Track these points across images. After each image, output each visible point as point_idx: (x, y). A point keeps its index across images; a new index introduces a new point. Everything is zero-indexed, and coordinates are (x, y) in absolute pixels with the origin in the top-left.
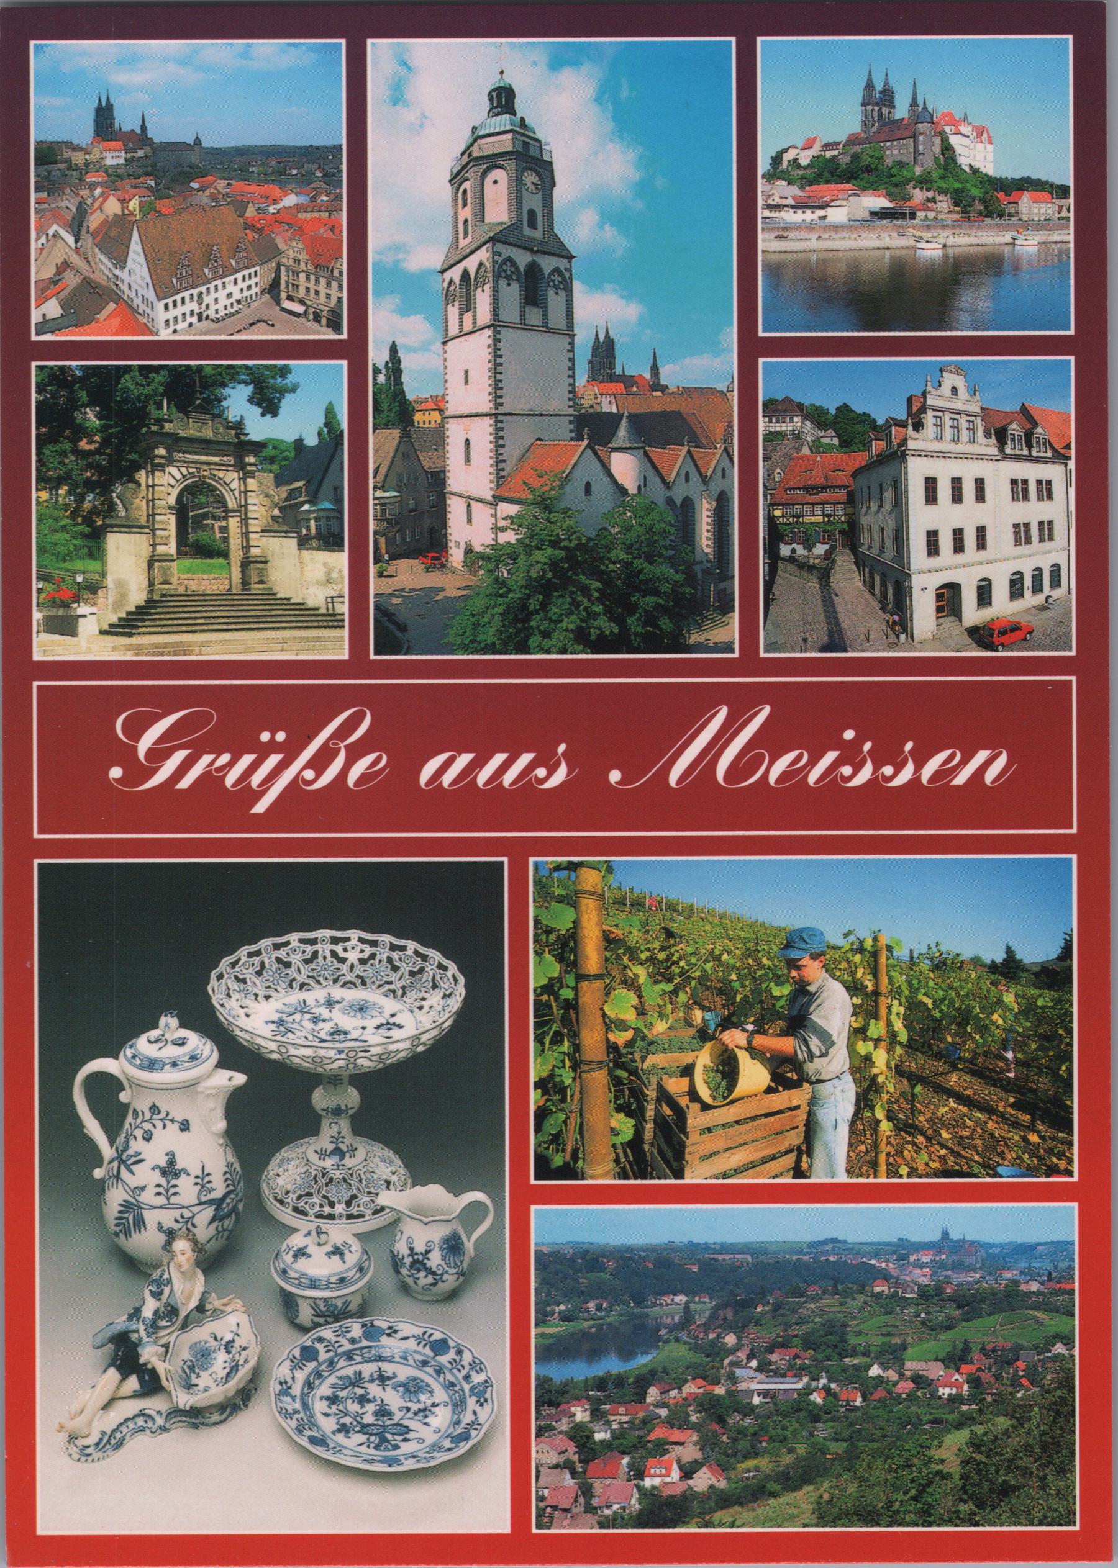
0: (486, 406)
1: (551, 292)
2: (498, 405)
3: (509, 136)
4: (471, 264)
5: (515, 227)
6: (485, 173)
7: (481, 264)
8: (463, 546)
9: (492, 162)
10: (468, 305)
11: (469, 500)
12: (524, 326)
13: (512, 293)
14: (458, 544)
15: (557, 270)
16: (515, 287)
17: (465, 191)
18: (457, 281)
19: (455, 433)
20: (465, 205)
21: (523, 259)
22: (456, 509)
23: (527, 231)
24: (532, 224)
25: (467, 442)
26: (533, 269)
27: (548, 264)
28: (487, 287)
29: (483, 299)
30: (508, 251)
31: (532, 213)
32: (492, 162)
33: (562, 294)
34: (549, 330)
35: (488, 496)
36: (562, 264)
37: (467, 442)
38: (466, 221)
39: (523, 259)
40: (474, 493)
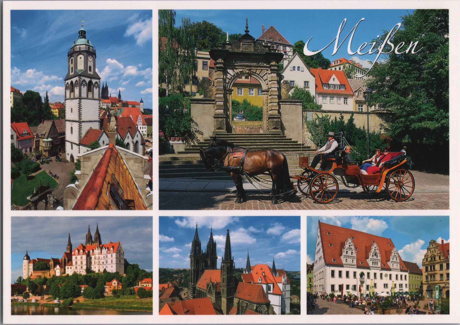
0: (77, 118)
1: (95, 88)
2: (80, 119)
3: (84, 46)
4: (74, 80)
5: (86, 71)
6: (77, 56)
7: (76, 81)
8: (70, 155)
9: (80, 52)
10: (72, 91)
11: (72, 143)
12: (87, 98)
13: (84, 89)
14: (68, 154)
15: (96, 83)
16: (86, 87)
17: (72, 60)
18: (69, 83)
19: (68, 125)
20: (72, 63)
21: (87, 80)
22: (68, 145)
23: (89, 72)
24: (90, 70)
25: (72, 128)
26: (90, 82)
27: (94, 81)
28: (78, 87)
29: (77, 90)
30: (83, 78)
31: (90, 67)
32: (80, 52)
33: (98, 89)
34: (95, 99)
35: (78, 143)
36: (97, 81)
37: (72, 128)
38: (72, 68)
39: (87, 80)
40: (74, 141)
